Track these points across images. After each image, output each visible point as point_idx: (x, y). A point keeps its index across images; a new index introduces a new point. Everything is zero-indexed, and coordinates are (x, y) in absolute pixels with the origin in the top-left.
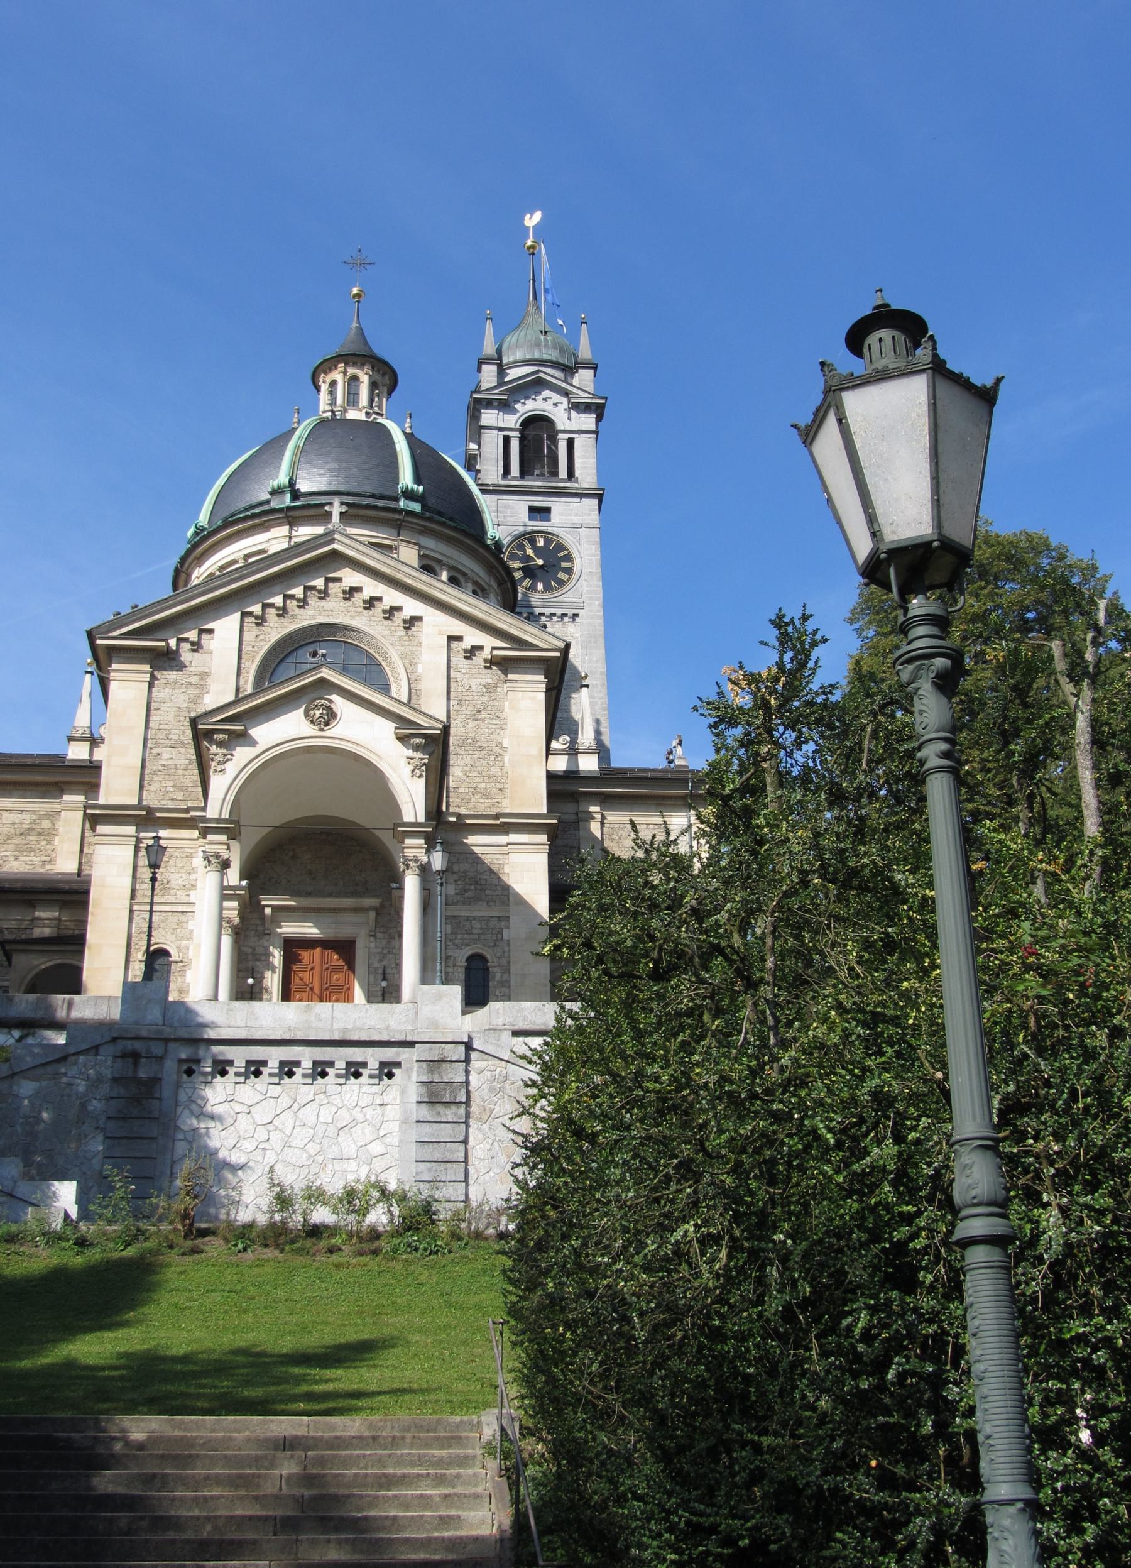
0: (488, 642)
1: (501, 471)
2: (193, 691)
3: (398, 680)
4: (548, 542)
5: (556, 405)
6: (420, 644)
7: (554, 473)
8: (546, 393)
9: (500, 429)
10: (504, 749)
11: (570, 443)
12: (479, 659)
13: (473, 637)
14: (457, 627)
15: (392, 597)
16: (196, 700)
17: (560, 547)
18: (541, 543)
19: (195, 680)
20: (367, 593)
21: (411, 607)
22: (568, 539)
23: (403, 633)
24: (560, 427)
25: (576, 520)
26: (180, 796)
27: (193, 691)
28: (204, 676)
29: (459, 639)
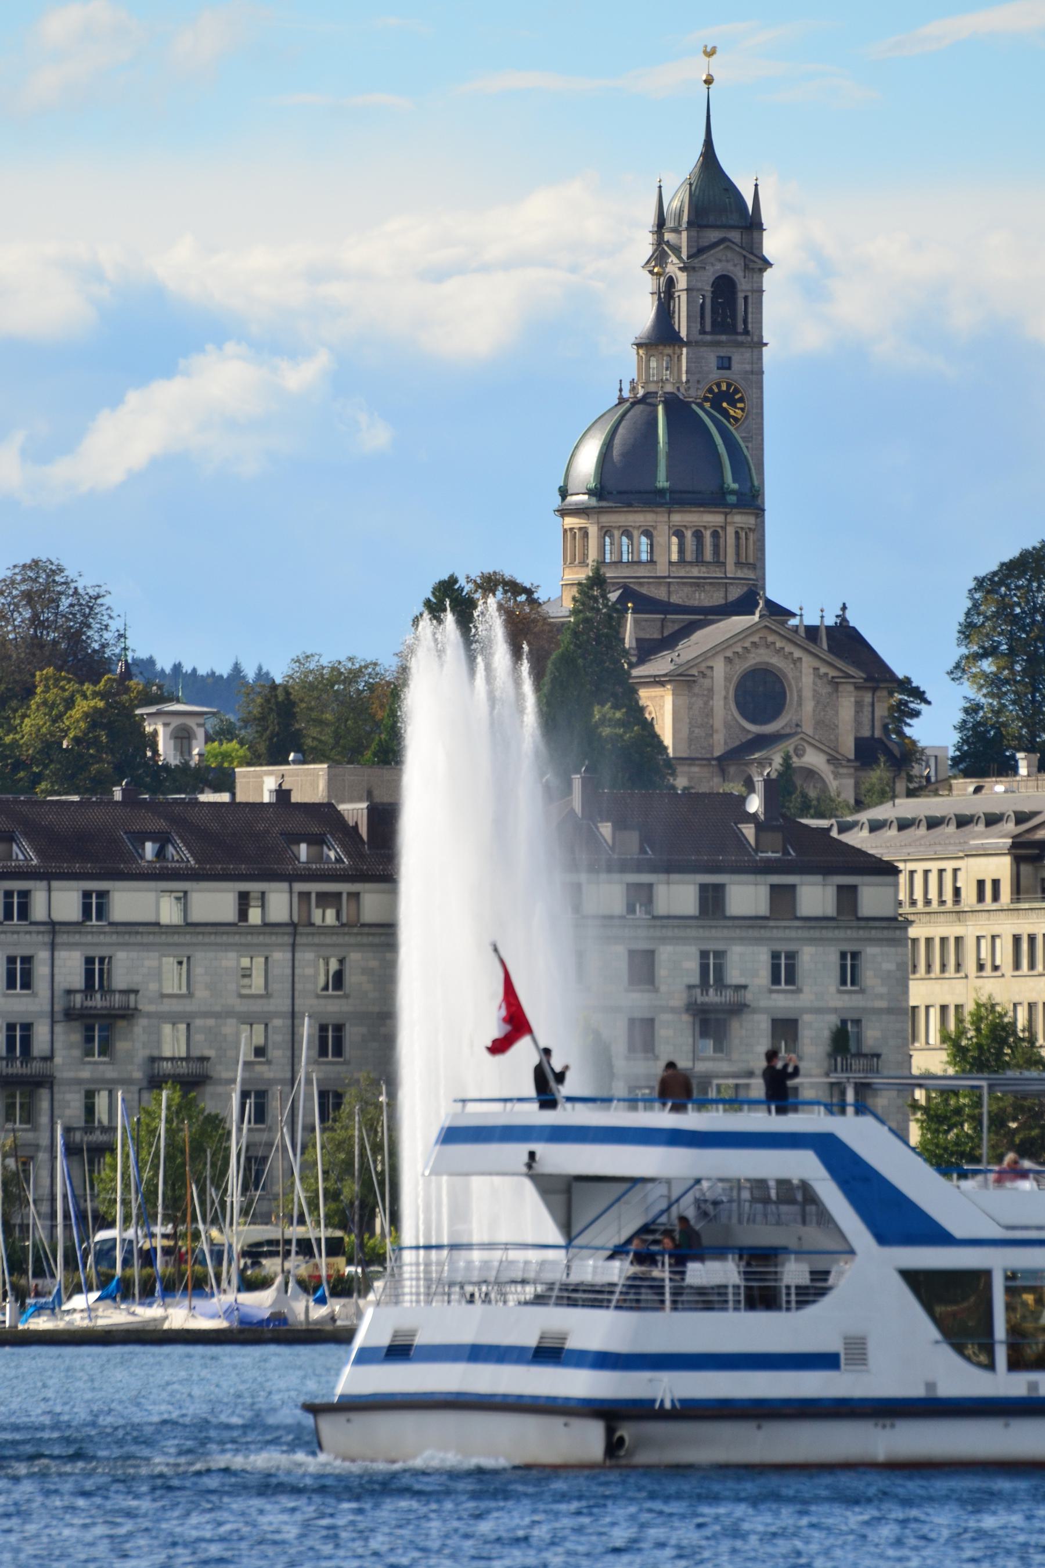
0: (832, 673)
1: (699, 327)
2: (705, 698)
3: (791, 691)
4: (729, 385)
5: (735, 265)
6: (801, 672)
7: (734, 325)
8: (730, 255)
9: (698, 290)
10: (837, 726)
11: (746, 298)
12: (825, 680)
13: (824, 670)
14: (817, 663)
15: (789, 648)
16: (706, 703)
17: (737, 391)
18: (724, 387)
19: (706, 693)
20: (778, 645)
21: (798, 653)
22: (741, 385)
23: (792, 666)
24: (739, 287)
25: (748, 367)
26: (703, 751)
27: (705, 698)
28: (711, 690)
29: (818, 669)
